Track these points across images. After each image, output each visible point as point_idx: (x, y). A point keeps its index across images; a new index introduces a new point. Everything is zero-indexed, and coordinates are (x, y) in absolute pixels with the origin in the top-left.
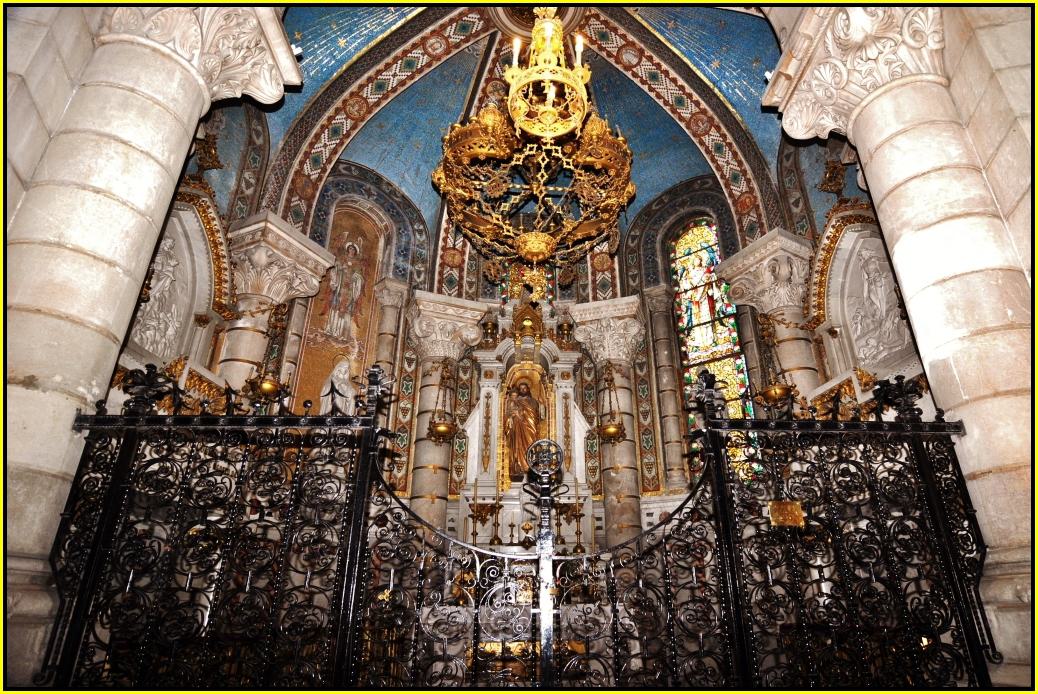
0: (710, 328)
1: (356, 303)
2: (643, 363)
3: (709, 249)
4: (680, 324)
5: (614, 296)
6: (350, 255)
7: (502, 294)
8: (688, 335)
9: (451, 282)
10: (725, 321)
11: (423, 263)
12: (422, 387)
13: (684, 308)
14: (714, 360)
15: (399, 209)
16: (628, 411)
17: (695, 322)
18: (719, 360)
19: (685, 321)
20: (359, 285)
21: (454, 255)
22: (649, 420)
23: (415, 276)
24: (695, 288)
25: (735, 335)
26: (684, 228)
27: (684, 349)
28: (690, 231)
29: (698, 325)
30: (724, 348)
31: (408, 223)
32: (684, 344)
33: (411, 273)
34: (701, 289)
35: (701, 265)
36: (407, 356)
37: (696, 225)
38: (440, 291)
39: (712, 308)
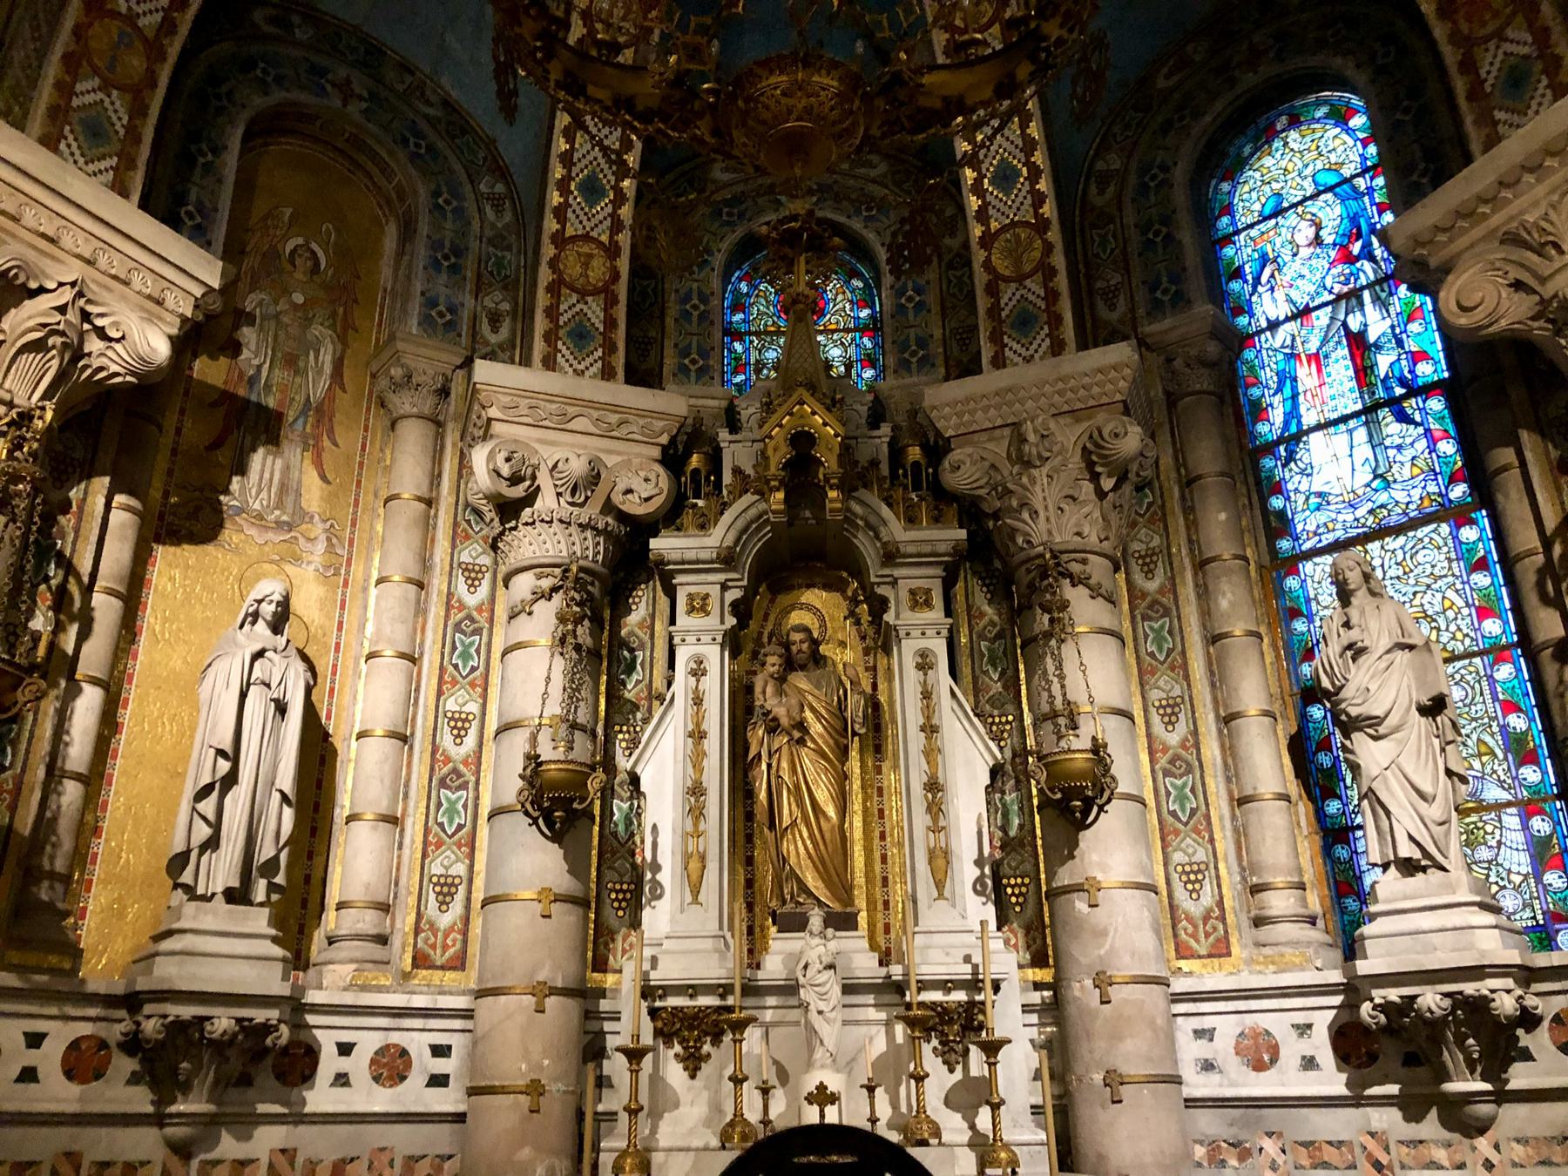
0: (1361, 434)
1: (319, 410)
2: (1151, 553)
3: (1341, 187)
4: (1262, 428)
5: (1057, 348)
6: (299, 275)
7: (736, 372)
8: (1291, 457)
9: (581, 336)
10: (1411, 405)
11: (505, 288)
12: (504, 654)
13: (1268, 376)
14: (1380, 533)
15: (432, 136)
16: (1119, 703)
17: (1309, 419)
18: (1398, 530)
19: (1277, 416)
20: (327, 358)
21: (590, 256)
22: (1182, 728)
23: (485, 328)
24: (1303, 313)
25: (1448, 447)
26: (1256, 139)
27: (1277, 502)
28: (1277, 144)
29: (1319, 427)
30: (1409, 493)
31: (464, 177)
32: (1278, 488)
33: (475, 318)
34: (1322, 318)
35: (1317, 241)
36: (465, 557)
37: (1295, 122)
38: (549, 363)
39: (1363, 373)
